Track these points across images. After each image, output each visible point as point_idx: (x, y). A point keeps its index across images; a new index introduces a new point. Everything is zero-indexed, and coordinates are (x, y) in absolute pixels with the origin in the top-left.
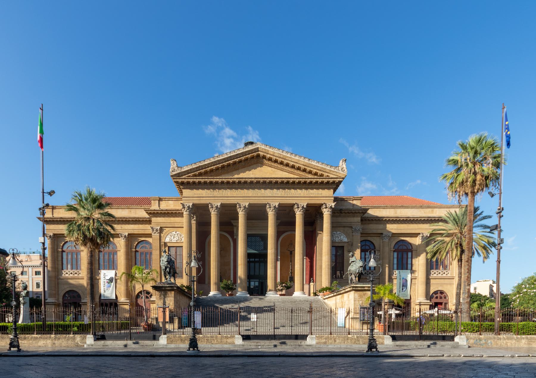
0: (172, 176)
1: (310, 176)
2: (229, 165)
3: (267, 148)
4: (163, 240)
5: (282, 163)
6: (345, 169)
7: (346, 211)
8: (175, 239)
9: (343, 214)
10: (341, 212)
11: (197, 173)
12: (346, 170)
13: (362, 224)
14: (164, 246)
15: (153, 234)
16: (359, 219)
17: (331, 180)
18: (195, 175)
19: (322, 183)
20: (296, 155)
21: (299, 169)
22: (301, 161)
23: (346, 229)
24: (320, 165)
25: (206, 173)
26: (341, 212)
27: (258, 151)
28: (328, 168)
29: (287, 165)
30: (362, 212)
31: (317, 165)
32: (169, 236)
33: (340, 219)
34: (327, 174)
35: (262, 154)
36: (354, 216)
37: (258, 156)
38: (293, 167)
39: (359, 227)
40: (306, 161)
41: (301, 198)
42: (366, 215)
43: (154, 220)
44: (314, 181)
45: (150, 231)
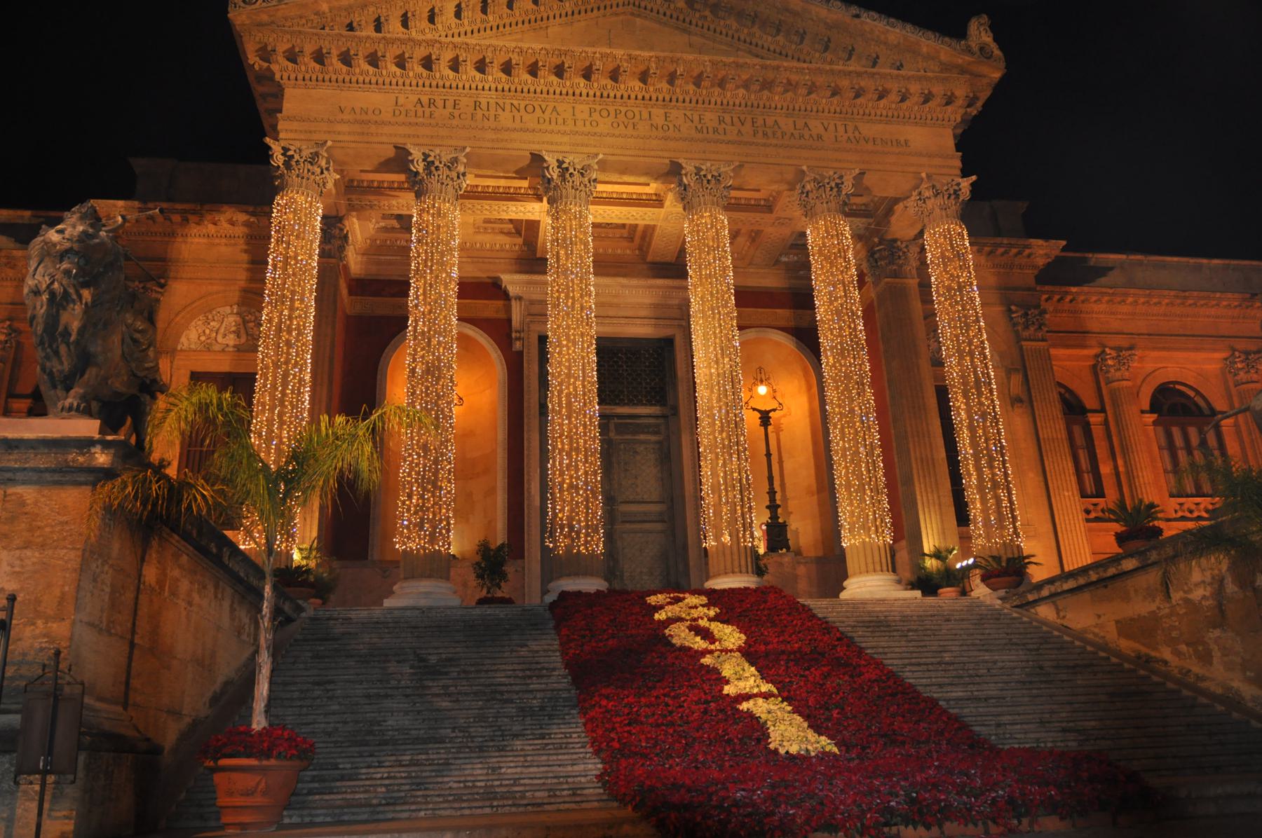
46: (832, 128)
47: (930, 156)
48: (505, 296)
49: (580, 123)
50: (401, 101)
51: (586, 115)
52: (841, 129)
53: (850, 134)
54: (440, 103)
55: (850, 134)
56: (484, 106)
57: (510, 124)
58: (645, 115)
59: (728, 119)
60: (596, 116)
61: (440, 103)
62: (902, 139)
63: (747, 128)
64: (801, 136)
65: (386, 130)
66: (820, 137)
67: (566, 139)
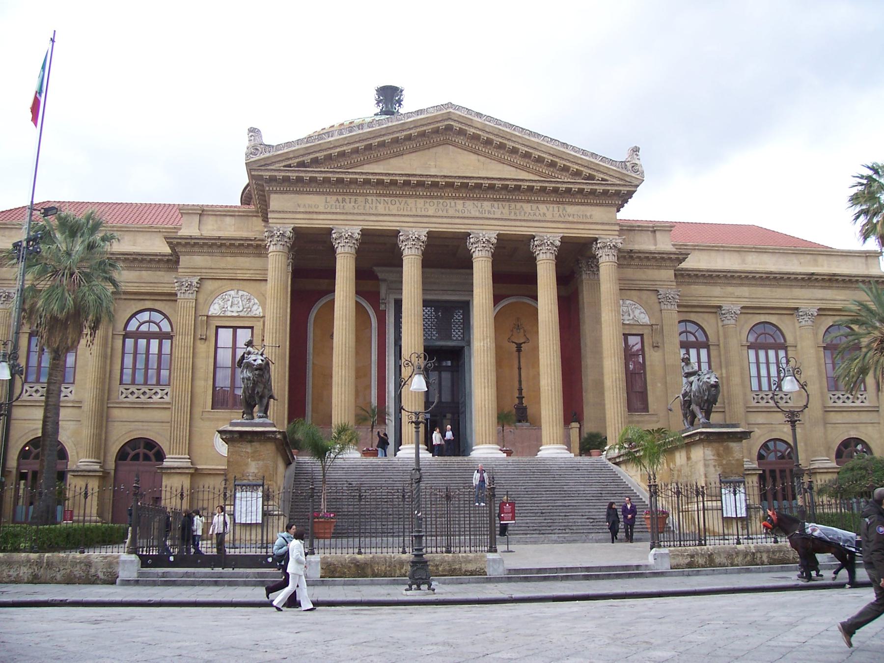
9: (636, 262)
10: (631, 257)
13: (679, 284)
16: (672, 272)
23: (645, 295)
30: (677, 259)
33: (630, 273)
36: (659, 267)
46: (551, 209)
47: (603, 224)
48: (376, 278)
49: (419, 210)
50: (329, 199)
51: (422, 205)
52: (556, 209)
53: (561, 212)
54: (348, 200)
55: (561, 212)
56: (370, 201)
57: (382, 211)
58: (453, 204)
59: (496, 205)
60: (427, 205)
61: (348, 200)
62: (588, 214)
63: (506, 211)
64: (535, 214)
65: (322, 216)
66: (544, 214)
67: (411, 219)
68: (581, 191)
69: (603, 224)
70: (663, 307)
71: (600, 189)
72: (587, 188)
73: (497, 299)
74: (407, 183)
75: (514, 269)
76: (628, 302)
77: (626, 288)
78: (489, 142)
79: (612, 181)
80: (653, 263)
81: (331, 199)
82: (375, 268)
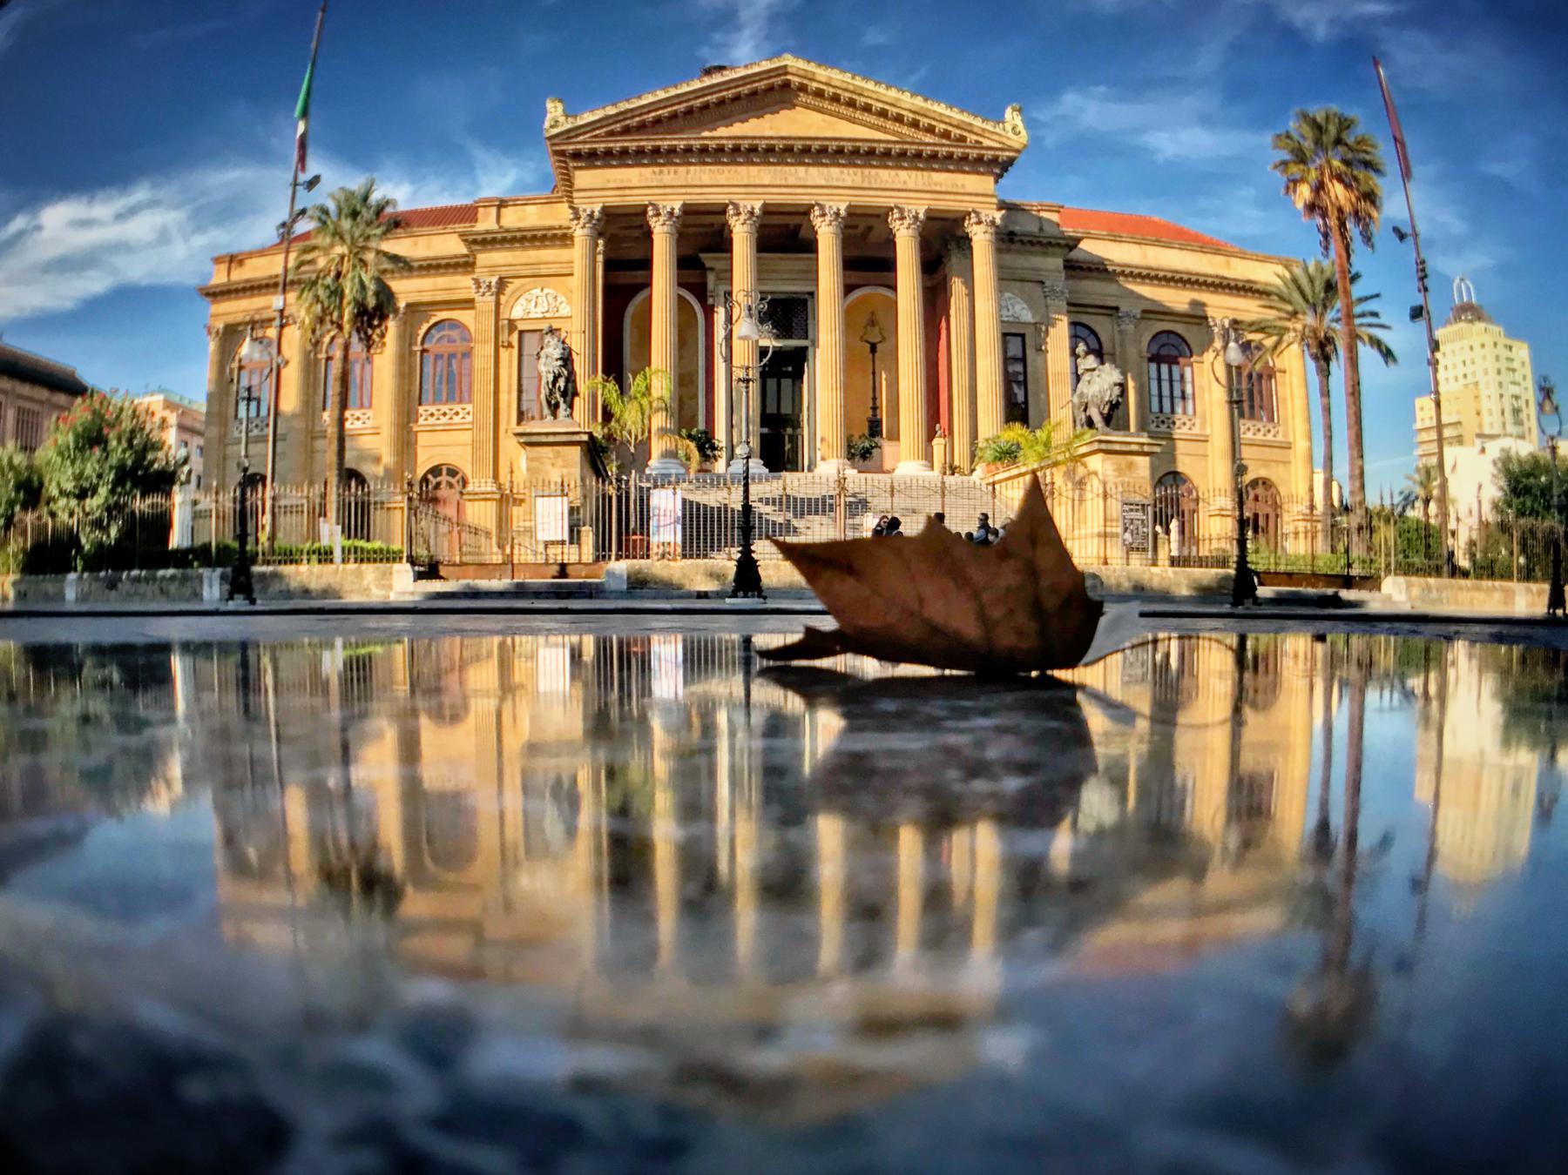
0: (550, 138)
1: (928, 139)
2: (706, 106)
3: (812, 67)
4: (504, 315)
5: (851, 104)
6: (1021, 127)
7: (1025, 239)
8: (540, 309)
9: (1017, 246)
11: (618, 127)
12: (1024, 133)
14: (508, 332)
15: (478, 298)
17: (989, 154)
18: (611, 133)
19: (964, 159)
20: (888, 87)
21: (899, 119)
22: (908, 101)
23: (1028, 287)
24: (956, 115)
25: (642, 127)
26: (1012, 241)
27: (787, 73)
28: (978, 122)
29: (867, 109)
31: (948, 112)
32: (522, 301)
33: (1009, 259)
34: (974, 137)
35: (796, 80)
36: (1045, 254)
37: (786, 85)
38: (883, 114)
39: (1059, 281)
40: (919, 102)
41: (908, 196)
42: (1074, 255)
43: (484, 258)
44: (943, 151)
45: (471, 293)
47: (977, 195)
68: (950, 157)
69: (977, 195)
70: (1049, 301)
71: (974, 153)
72: (958, 152)
73: (848, 289)
74: (736, 149)
75: (867, 258)
76: (1007, 295)
77: (1006, 278)
78: (835, 99)
79: (986, 143)
80: (1037, 248)
81: (647, 171)
82: (702, 255)
